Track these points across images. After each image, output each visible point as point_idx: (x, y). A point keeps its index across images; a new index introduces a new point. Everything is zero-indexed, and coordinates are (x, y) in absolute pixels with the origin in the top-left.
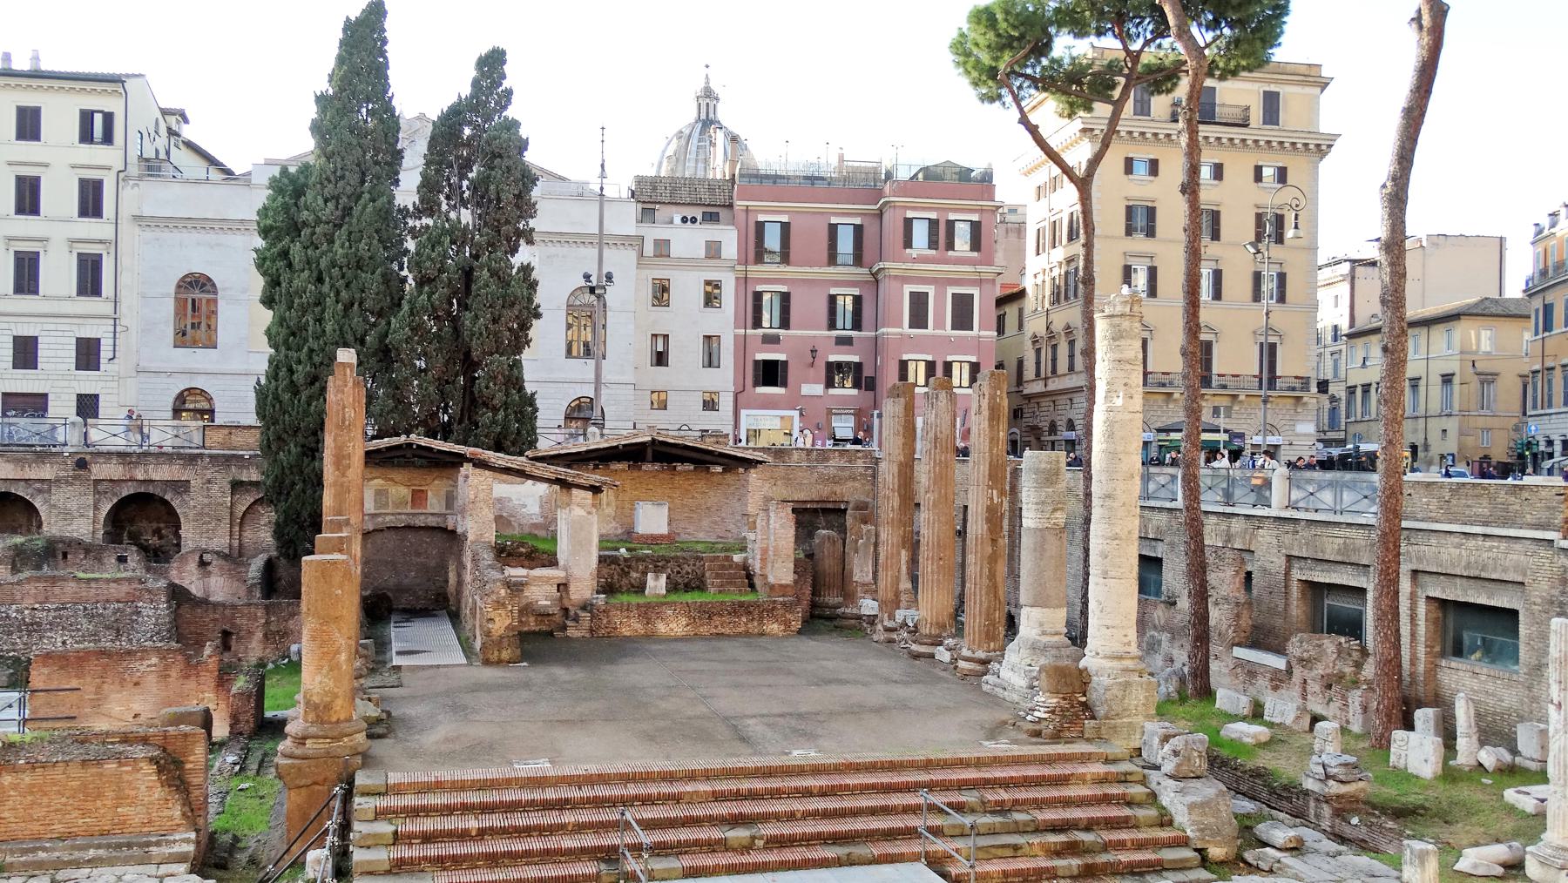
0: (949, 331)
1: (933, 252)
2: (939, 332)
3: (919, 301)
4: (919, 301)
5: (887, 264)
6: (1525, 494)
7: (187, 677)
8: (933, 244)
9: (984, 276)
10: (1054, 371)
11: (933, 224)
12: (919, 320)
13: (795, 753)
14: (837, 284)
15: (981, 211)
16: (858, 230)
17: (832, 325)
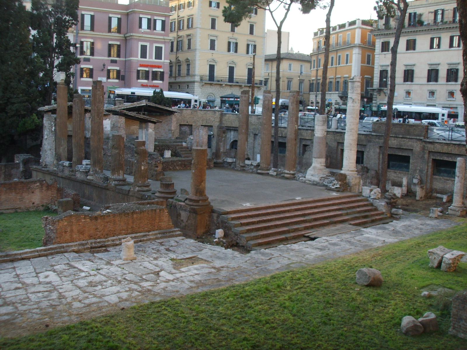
0: (154, 59)
1: (149, 30)
2: (150, 60)
3: (144, 48)
4: (144, 48)
5: (134, 34)
6: (414, 128)
7: (48, 189)
8: (149, 27)
9: (166, 40)
10: (179, 75)
11: (149, 20)
12: (144, 55)
13: (297, 198)
14: (112, 40)
15: (165, 16)
16: (119, 20)
17: (109, 55)
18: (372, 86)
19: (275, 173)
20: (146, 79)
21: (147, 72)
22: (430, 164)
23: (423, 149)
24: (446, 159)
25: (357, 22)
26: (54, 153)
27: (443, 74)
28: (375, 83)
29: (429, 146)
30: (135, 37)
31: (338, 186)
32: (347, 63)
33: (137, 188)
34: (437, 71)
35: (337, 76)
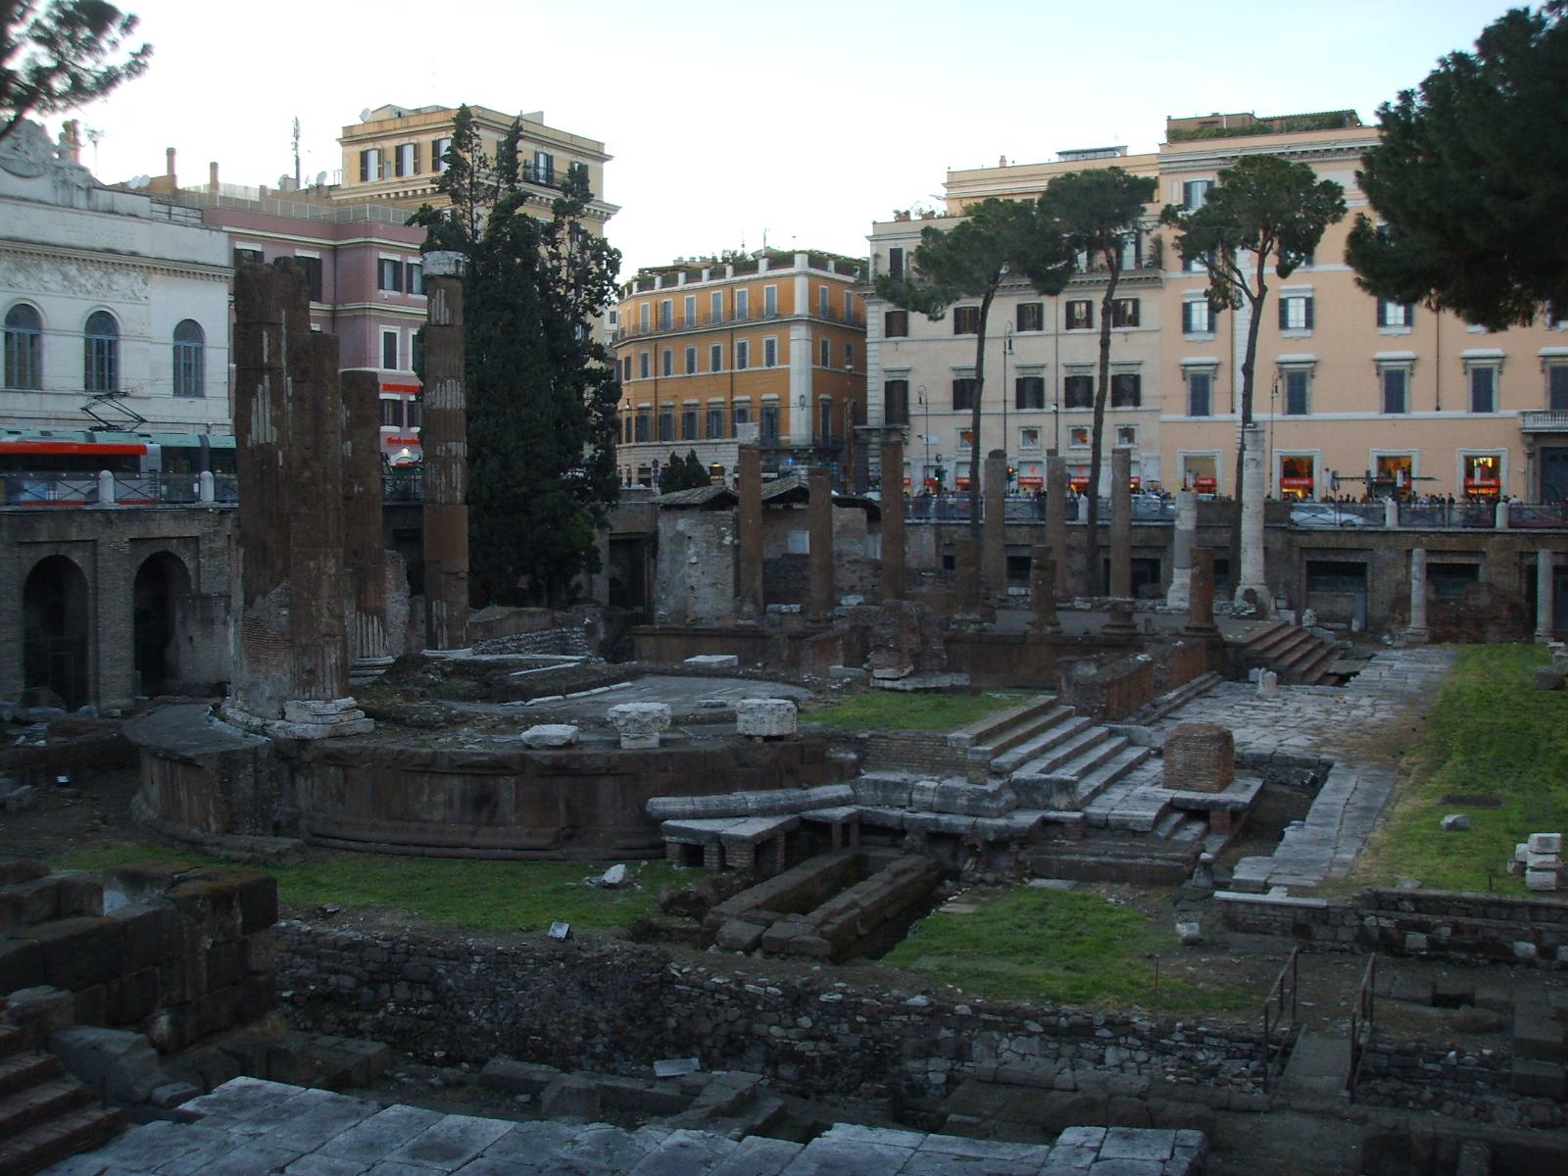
1: (398, 294)
3: (390, 338)
4: (390, 338)
18: (865, 423)
19: (1088, 606)
20: (395, 424)
21: (397, 404)
22: (1304, 571)
23: (1289, 544)
24: (1332, 558)
25: (798, 259)
26: (730, 591)
27: (1054, 389)
28: (870, 414)
29: (1300, 538)
30: (373, 313)
31: (1253, 610)
32: (770, 362)
33: (1049, 629)
34: (1039, 383)
35: (736, 399)
